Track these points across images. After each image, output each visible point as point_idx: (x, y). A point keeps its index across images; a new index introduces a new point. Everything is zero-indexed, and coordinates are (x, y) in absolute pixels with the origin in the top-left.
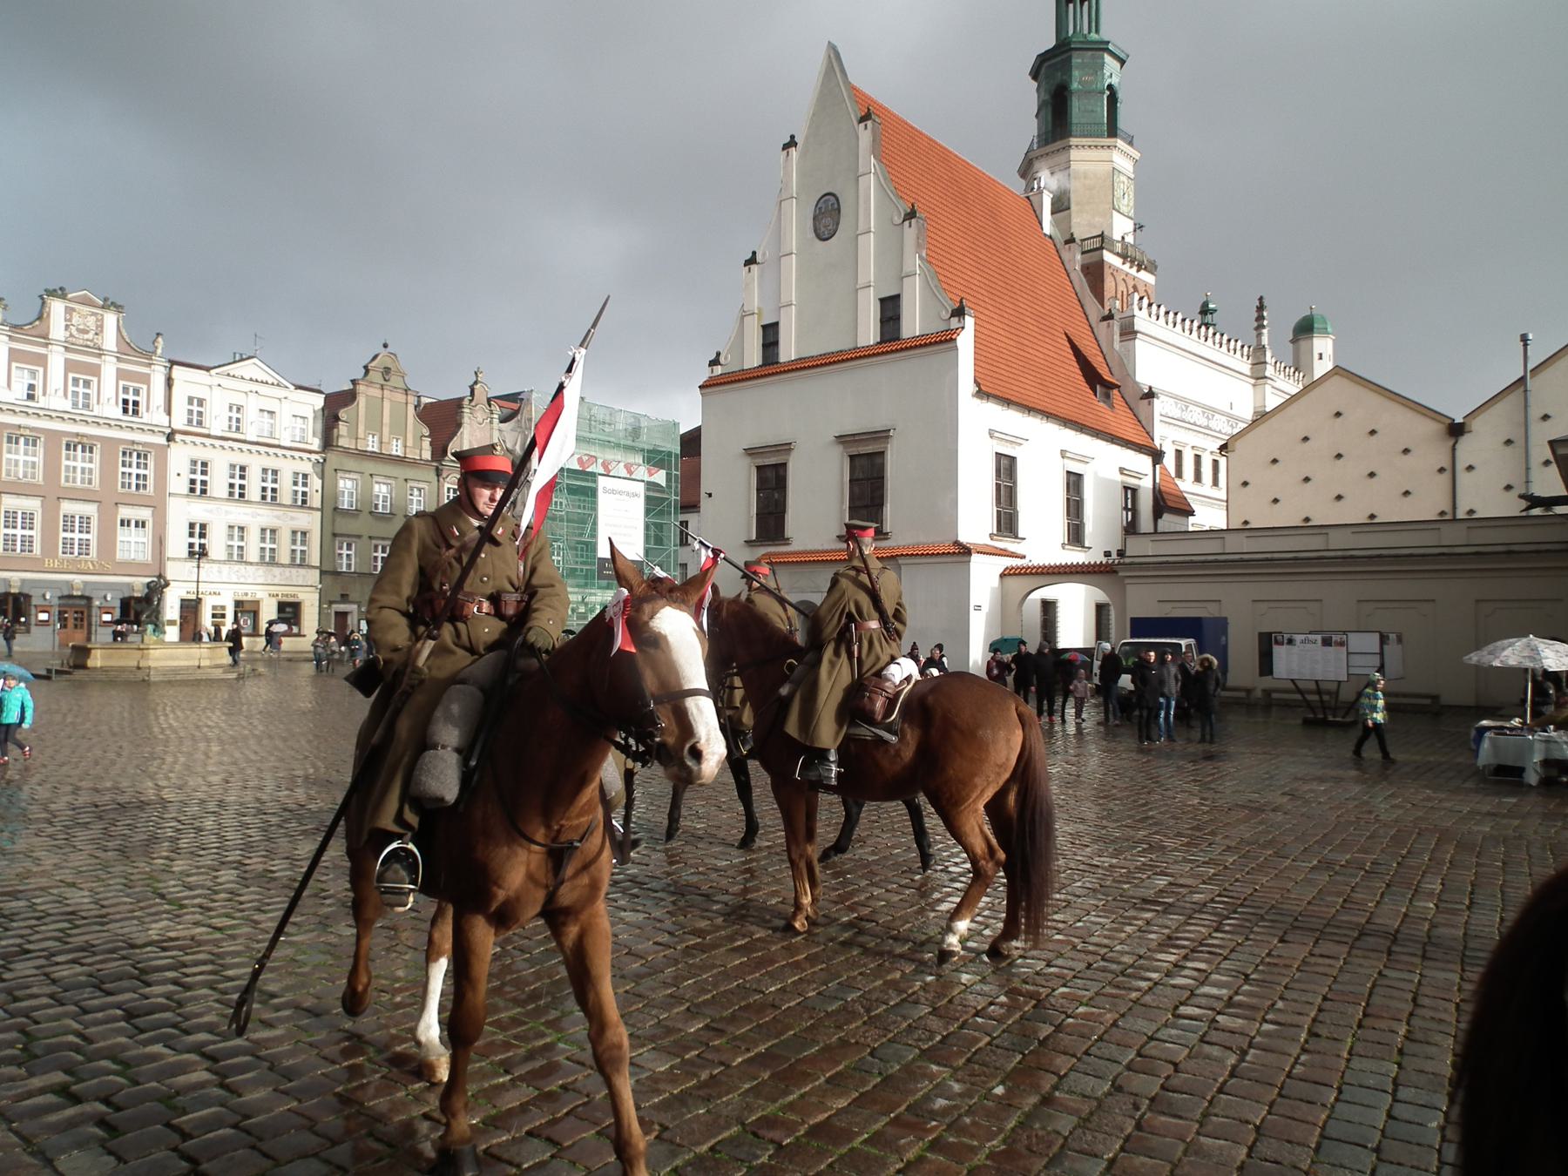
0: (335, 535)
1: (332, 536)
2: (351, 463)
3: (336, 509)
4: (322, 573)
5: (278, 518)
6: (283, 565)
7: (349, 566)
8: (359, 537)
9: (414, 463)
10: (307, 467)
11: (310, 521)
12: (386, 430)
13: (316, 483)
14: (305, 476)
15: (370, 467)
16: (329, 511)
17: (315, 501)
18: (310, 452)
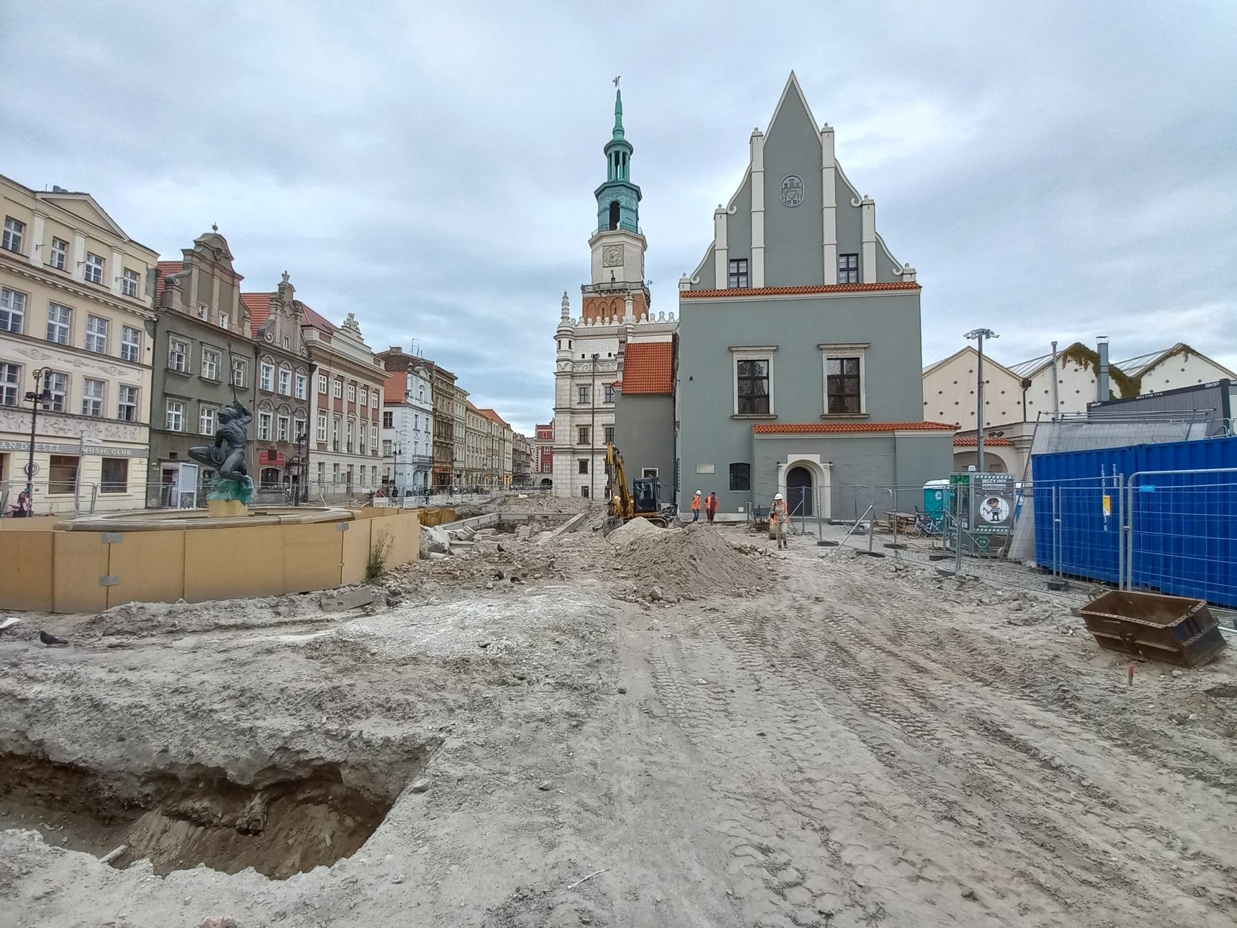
0: (166, 395)
1: (162, 397)
2: (182, 329)
3: (167, 370)
4: (152, 431)
5: (105, 370)
6: (110, 421)
7: (176, 426)
8: (189, 399)
9: (239, 339)
10: (140, 324)
11: (143, 380)
12: (215, 304)
13: (149, 342)
14: (136, 332)
15: (200, 336)
16: (160, 369)
17: (147, 359)
18: (145, 309)
